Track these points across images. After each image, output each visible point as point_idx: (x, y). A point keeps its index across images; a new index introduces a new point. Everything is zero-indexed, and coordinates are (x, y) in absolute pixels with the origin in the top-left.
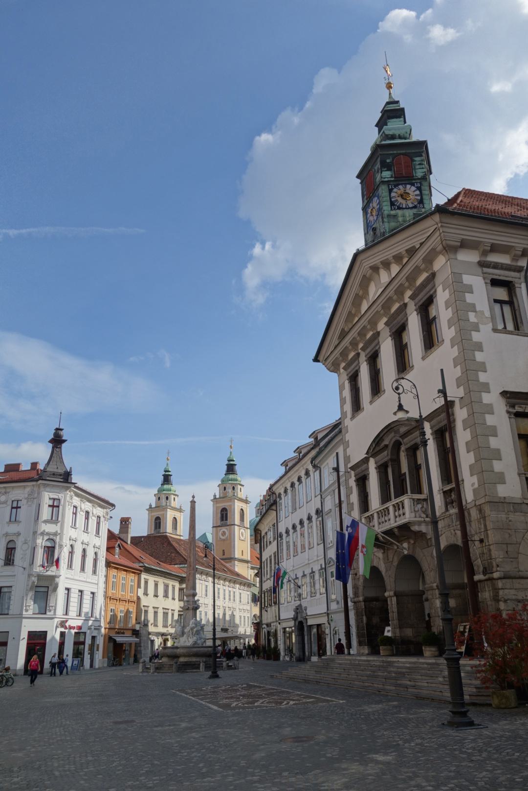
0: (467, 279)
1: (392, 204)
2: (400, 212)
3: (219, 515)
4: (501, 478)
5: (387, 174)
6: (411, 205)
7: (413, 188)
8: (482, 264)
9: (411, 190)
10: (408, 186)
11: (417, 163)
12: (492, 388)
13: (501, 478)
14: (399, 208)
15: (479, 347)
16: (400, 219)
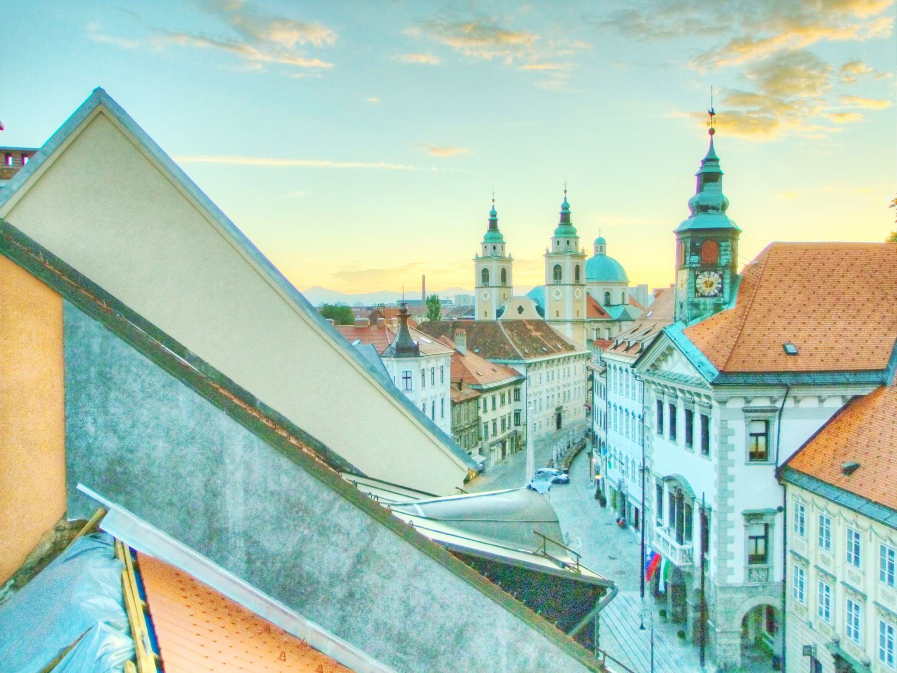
0: (731, 424)
1: (696, 291)
2: (702, 300)
3: (552, 273)
4: (731, 571)
5: (695, 259)
6: (712, 294)
7: (717, 276)
8: (745, 411)
9: (714, 277)
10: (712, 273)
11: (723, 248)
12: (736, 508)
13: (731, 571)
14: (702, 296)
15: (732, 479)
16: (702, 307)
